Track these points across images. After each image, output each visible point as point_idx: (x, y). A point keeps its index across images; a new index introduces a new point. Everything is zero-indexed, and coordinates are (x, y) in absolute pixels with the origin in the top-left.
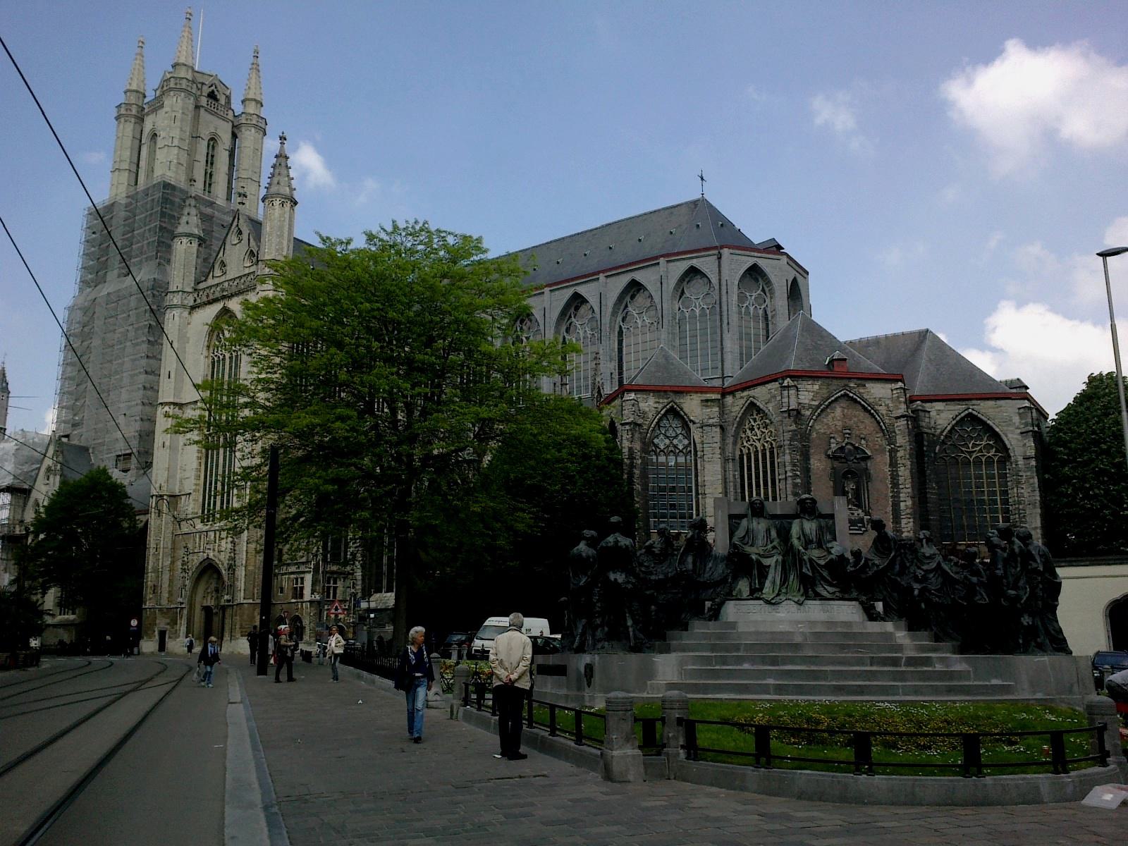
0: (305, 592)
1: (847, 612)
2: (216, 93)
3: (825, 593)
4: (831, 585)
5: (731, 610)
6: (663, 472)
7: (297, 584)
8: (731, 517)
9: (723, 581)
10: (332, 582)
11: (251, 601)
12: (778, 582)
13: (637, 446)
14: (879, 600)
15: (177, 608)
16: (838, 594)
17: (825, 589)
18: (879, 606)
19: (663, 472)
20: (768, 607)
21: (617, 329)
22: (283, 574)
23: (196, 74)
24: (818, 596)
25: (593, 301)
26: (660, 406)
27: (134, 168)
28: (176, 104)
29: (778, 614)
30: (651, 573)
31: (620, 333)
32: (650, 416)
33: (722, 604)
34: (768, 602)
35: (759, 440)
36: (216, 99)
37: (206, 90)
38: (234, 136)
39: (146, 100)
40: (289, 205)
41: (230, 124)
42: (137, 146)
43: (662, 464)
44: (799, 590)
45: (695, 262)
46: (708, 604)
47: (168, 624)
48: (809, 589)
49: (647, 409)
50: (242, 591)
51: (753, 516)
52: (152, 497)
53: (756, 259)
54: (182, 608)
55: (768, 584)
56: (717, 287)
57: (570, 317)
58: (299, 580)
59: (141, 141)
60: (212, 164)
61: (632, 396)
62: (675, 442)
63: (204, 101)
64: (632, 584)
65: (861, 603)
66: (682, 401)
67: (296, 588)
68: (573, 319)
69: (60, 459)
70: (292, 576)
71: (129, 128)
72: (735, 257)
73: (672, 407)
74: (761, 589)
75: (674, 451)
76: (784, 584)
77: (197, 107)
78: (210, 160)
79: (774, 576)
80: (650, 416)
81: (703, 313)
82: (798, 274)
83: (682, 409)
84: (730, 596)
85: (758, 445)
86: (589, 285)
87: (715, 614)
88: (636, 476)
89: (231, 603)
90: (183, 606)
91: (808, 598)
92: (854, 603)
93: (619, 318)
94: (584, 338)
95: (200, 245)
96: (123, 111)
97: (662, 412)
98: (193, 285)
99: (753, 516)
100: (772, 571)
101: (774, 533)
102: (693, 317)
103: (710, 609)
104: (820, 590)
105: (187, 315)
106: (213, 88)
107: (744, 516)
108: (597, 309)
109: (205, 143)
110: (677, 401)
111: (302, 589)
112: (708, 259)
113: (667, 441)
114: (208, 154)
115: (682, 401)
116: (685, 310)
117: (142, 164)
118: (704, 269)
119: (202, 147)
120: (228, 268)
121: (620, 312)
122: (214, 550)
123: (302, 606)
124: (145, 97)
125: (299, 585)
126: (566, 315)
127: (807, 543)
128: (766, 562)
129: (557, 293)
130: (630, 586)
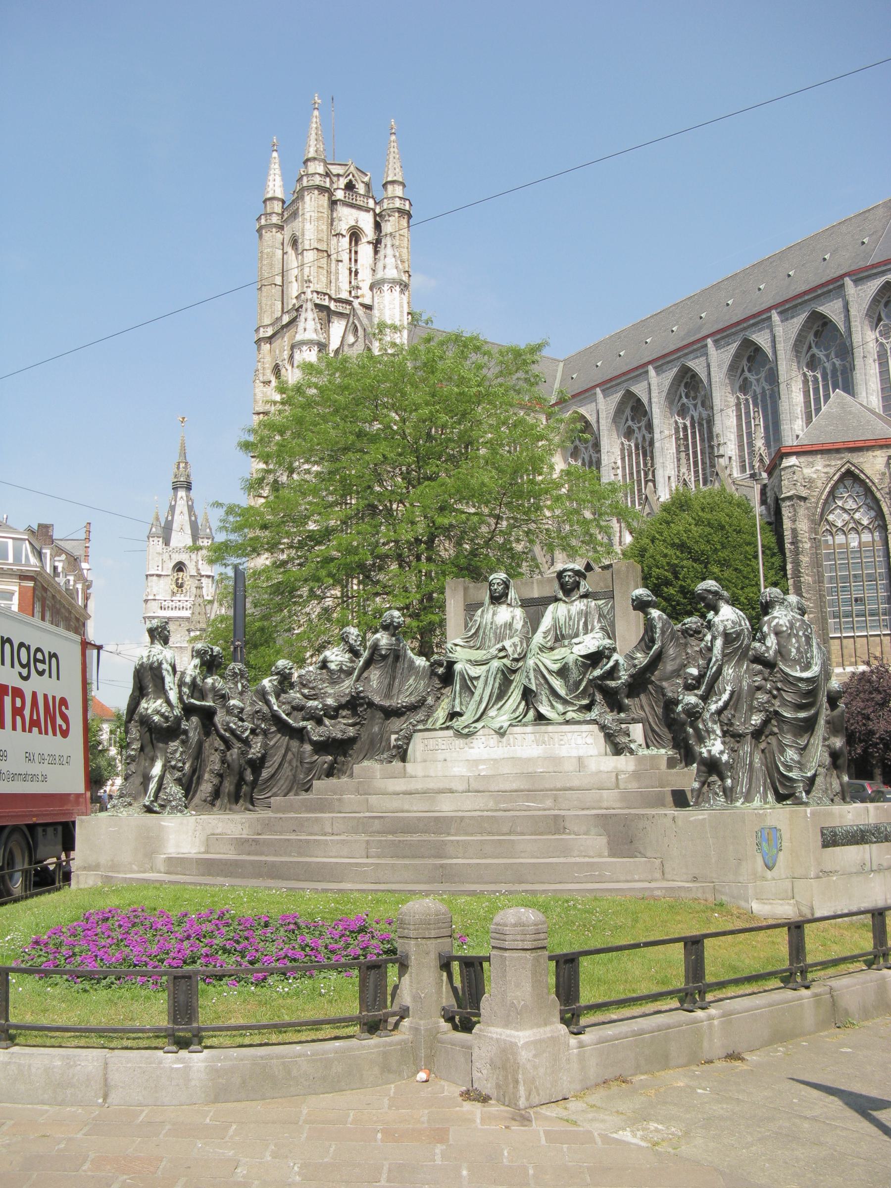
4: (565, 702)
5: (418, 746)
6: (868, 554)
13: (803, 526)
14: (635, 721)
17: (553, 707)
18: (637, 731)
19: (868, 554)
20: (460, 742)
23: (329, 167)
26: (832, 471)
28: (313, 204)
29: (472, 751)
30: (314, 697)
32: (819, 484)
33: (409, 738)
37: (343, 182)
38: (378, 226)
40: (398, 288)
41: (371, 213)
43: (840, 546)
44: (515, 711)
49: (815, 476)
55: (473, 705)
61: (793, 460)
62: (857, 516)
63: (340, 195)
64: (162, 715)
65: (603, 728)
66: (861, 460)
75: (858, 527)
77: (333, 203)
79: (484, 690)
80: (819, 484)
83: (862, 471)
87: (402, 755)
88: (803, 565)
91: (518, 721)
95: (320, 351)
96: (263, 222)
97: (836, 478)
100: (480, 684)
101: (518, 625)
104: (544, 710)
106: (351, 176)
109: (347, 239)
110: (855, 461)
113: (846, 517)
115: (861, 460)
116: (884, 341)
128: (474, 671)
130: (156, 718)
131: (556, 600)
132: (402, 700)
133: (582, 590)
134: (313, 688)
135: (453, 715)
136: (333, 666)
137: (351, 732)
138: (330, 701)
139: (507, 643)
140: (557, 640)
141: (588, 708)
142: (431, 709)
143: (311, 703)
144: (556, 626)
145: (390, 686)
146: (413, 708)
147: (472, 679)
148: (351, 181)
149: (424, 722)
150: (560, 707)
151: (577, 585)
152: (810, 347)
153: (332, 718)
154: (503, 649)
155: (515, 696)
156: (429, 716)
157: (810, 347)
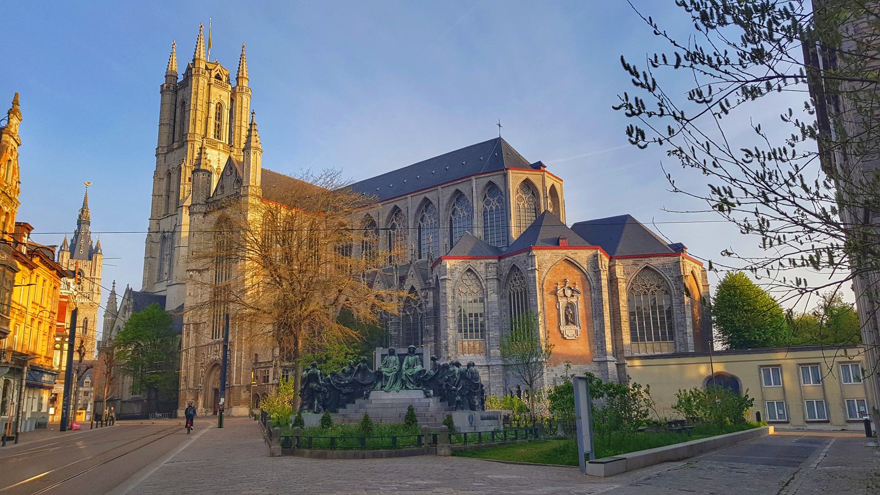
1: (415, 395)
2: (220, 75)
4: (413, 384)
8: (382, 355)
9: (373, 382)
11: (239, 385)
16: (415, 387)
18: (432, 392)
21: (449, 219)
22: (257, 368)
24: (407, 388)
25: (435, 202)
27: (172, 123)
31: (451, 220)
33: (370, 392)
34: (386, 391)
35: (519, 286)
36: (221, 79)
45: (491, 179)
46: (365, 392)
48: (404, 386)
50: (234, 379)
51: (390, 355)
53: (527, 175)
54: (201, 390)
55: (388, 384)
56: (504, 193)
57: (423, 212)
63: (213, 80)
70: (263, 370)
71: (168, 97)
72: (515, 175)
73: (469, 270)
74: (385, 386)
77: (209, 85)
78: (219, 117)
79: (391, 380)
81: (497, 209)
82: (555, 183)
85: (518, 289)
86: (432, 193)
87: (367, 396)
91: (401, 389)
99: (390, 355)
100: (390, 378)
101: (398, 362)
102: (491, 210)
106: (218, 72)
107: (387, 355)
111: (268, 376)
112: (498, 176)
117: (177, 120)
118: (497, 183)
119: (213, 107)
120: (225, 190)
121: (451, 207)
122: (219, 355)
127: (409, 366)
128: (388, 375)
129: (414, 198)
130: (317, 388)
131: (406, 355)
132: (366, 382)
135: (382, 387)
137: (352, 391)
141: (418, 386)
143: (343, 382)
144: (408, 364)
146: (370, 384)
148: (218, 74)
149: (374, 388)
151: (414, 351)
152: (454, 205)
153: (347, 386)
154: (395, 368)
155: (399, 382)
156: (375, 386)
157: (454, 205)
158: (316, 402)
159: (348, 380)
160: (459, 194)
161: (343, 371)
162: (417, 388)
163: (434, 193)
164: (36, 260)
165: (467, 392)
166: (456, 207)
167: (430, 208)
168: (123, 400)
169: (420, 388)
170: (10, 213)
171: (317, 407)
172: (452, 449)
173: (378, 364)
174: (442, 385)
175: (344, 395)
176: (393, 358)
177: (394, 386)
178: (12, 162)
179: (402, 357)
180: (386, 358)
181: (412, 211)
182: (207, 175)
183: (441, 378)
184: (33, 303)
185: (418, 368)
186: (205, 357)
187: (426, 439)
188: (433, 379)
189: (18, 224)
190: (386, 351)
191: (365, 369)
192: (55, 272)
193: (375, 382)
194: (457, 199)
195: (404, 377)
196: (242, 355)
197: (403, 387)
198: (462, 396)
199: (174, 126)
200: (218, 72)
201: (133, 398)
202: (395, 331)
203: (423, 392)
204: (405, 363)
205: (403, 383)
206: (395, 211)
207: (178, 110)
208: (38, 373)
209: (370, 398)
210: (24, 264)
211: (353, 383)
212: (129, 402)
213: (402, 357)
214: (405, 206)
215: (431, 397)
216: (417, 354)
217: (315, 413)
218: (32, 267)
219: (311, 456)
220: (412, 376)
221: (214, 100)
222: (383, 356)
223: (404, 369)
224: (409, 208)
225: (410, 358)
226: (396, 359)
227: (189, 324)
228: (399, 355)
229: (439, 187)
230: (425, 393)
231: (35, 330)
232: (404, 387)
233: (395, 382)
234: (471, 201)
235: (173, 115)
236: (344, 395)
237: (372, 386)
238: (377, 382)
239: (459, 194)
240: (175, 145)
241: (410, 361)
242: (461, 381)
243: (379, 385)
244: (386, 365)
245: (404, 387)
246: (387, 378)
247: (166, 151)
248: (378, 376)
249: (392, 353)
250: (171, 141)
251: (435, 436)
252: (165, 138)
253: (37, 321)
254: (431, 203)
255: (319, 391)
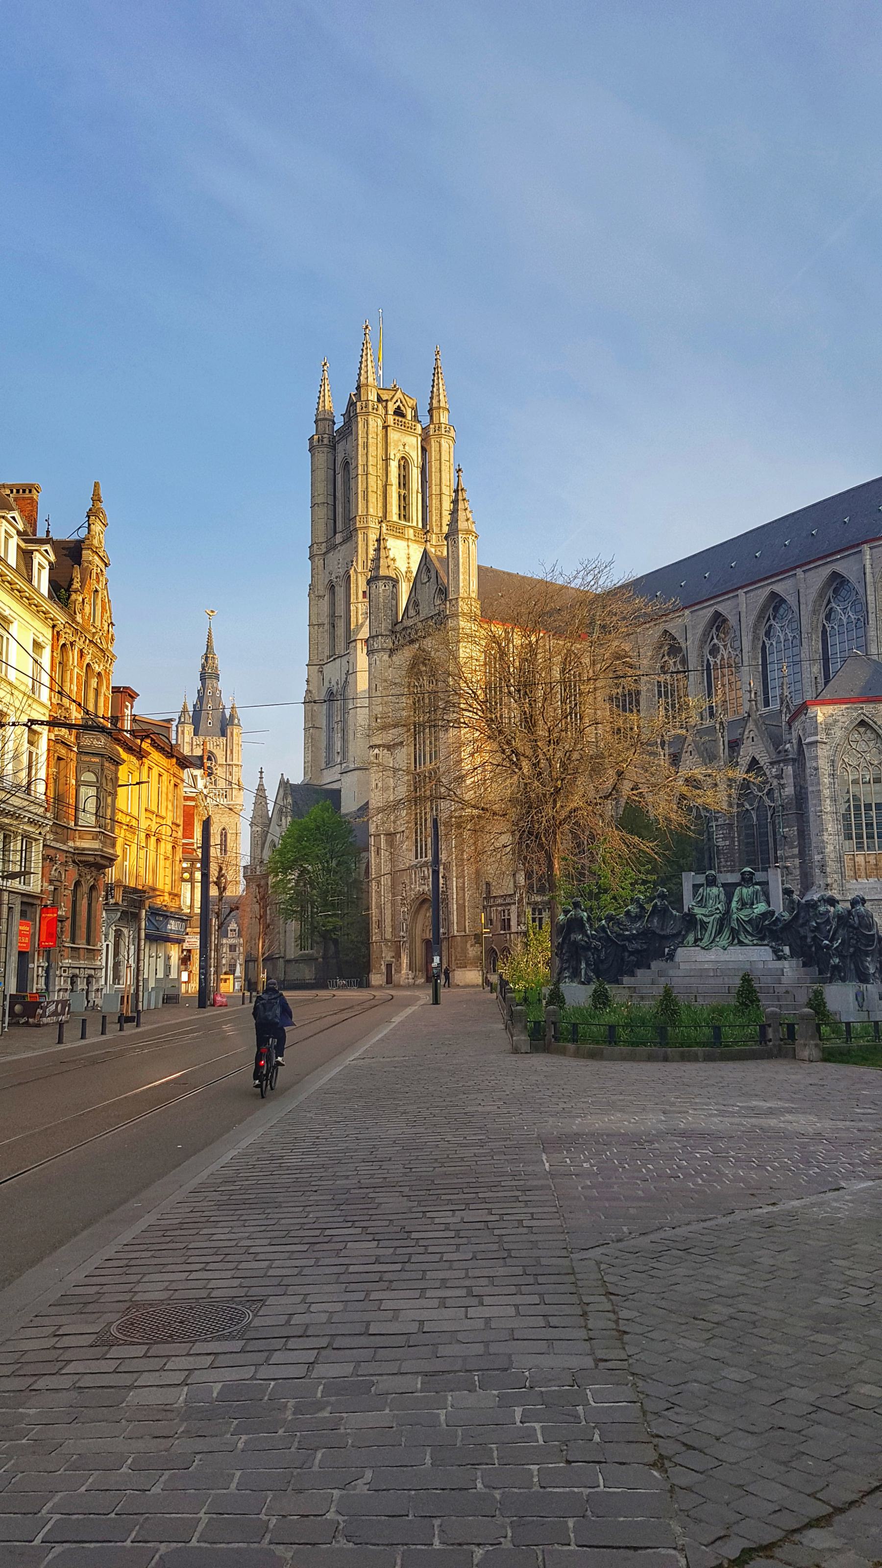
0: (512, 924)
2: (402, 408)
3: (746, 941)
4: (751, 935)
7: (504, 916)
8: (694, 886)
10: (537, 913)
11: (463, 933)
12: (713, 935)
15: (400, 941)
16: (755, 942)
18: (787, 949)
21: (820, 629)
22: (491, 907)
24: (741, 943)
25: (791, 600)
27: (330, 500)
31: (824, 632)
33: (675, 950)
34: (703, 948)
36: (403, 416)
39: (336, 428)
42: (332, 477)
46: (667, 950)
47: (393, 957)
48: (735, 939)
50: (455, 924)
51: (707, 885)
52: (371, 836)
54: (404, 942)
55: (707, 935)
57: (769, 619)
58: (506, 911)
59: (335, 472)
60: (404, 485)
63: (391, 419)
64: (586, 941)
65: (771, 947)
67: (504, 919)
68: (772, 622)
69: (290, 800)
70: (499, 908)
71: (322, 457)
74: (701, 939)
76: (718, 935)
77: (385, 428)
78: (404, 482)
79: (712, 928)
84: (681, 944)
86: (786, 582)
87: (671, 957)
89: (446, 936)
90: (405, 939)
91: (731, 944)
92: (767, 947)
93: (822, 616)
94: (785, 641)
98: (390, 628)
99: (707, 885)
100: (710, 926)
101: (722, 897)
103: (668, 954)
105: (388, 659)
106: (399, 403)
107: (702, 885)
108: (795, 609)
111: (509, 920)
114: (399, 475)
117: (339, 494)
119: (394, 466)
120: (421, 608)
121: (823, 608)
122: (428, 885)
123: (510, 937)
124: (334, 423)
125: (506, 917)
126: (764, 618)
127: (743, 904)
128: (706, 919)
129: (752, 594)
130: (583, 943)
132: (668, 931)
133: (754, 881)
134: (625, 925)
135: (696, 940)
136: (633, 915)
138: (634, 932)
139: (719, 906)
140: (743, 905)
141: (762, 939)
142: (684, 937)
143: (627, 933)
144: (741, 899)
145: (663, 925)
146: (675, 936)
147: (705, 923)
148: (399, 407)
149: (682, 942)
150: (750, 938)
151: (751, 879)
152: (829, 602)
154: (718, 909)
155: (726, 933)
157: (829, 602)
158: (583, 966)
159: (637, 929)
160: (838, 581)
161: (628, 913)
162: (760, 943)
163: (789, 583)
164: (146, 745)
165: (852, 950)
166: (833, 605)
167: (781, 611)
168: (287, 958)
169: (766, 942)
170: (103, 673)
171: (586, 974)
172: (823, 1050)
173: (688, 901)
174: (806, 937)
175: (632, 953)
176: (715, 890)
177: (717, 940)
178: (100, 593)
179: (729, 889)
180: (701, 890)
181: (748, 621)
182: (391, 585)
183: (803, 925)
184: (146, 810)
185: (760, 908)
186: (408, 888)
187: (774, 1032)
188: (788, 926)
189: (116, 690)
190: (701, 879)
191: (665, 910)
192: (174, 760)
193: (683, 933)
194: (835, 591)
195: (734, 924)
196: (464, 884)
197: (733, 940)
198: (842, 957)
199: (334, 505)
200: (399, 403)
201: (302, 955)
202: (724, 839)
203: (771, 950)
204: (735, 899)
205: (734, 933)
206: (715, 622)
207: (339, 478)
208: (161, 919)
209: (677, 959)
210: (130, 750)
211: (645, 934)
212: (296, 961)
213: (729, 889)
214: (734, 612)
215: (785, 959)
216: (757, 884)
217: (583, 983)
218: (141, 755)
219: (577, 1055)
220: (749, 922)
221: (395, 454)
222: (696, 887)
223: (735, 910)
224: (743, 615)
225: (745, 890)
226: (720, 892)
227: (379, 835)
228: (724, 885)
229: (799, 571)
230: (775, 951)
231: (152, 855)
232: (736, 941)
233: (719, 932)
234: (861, 591)
235: (331, 486)
236: (632, 953)
237: (678, 939)
238: (687, 932)
239: (838, 581)
240: (339, 538)
241: (745, 896)
242: (840, 931)
243: (691, 938)
244: (702, 903)
245: (736, 941)
246: (704, 926)
247: (324, 550)
248: (688, 922)
249: (711, 882)
250: (331, 532)
251: (791, 1027)
252: (321, 527)
253: (153, 839)
254: (783, 601)
255: (587, 947)
